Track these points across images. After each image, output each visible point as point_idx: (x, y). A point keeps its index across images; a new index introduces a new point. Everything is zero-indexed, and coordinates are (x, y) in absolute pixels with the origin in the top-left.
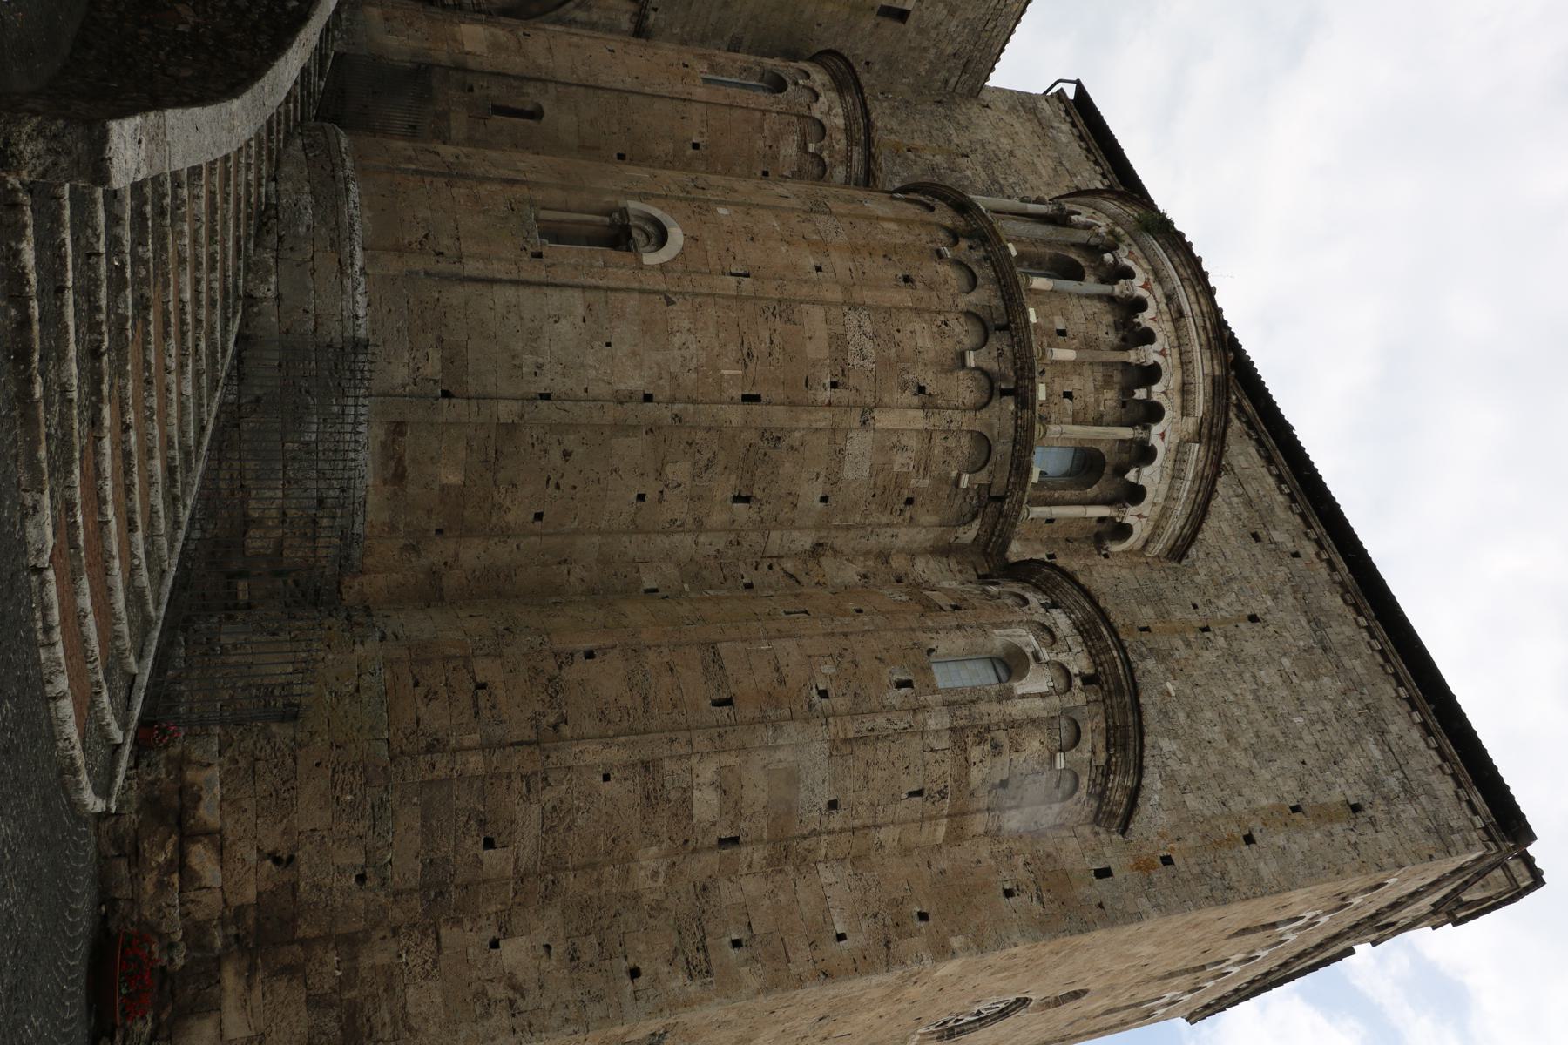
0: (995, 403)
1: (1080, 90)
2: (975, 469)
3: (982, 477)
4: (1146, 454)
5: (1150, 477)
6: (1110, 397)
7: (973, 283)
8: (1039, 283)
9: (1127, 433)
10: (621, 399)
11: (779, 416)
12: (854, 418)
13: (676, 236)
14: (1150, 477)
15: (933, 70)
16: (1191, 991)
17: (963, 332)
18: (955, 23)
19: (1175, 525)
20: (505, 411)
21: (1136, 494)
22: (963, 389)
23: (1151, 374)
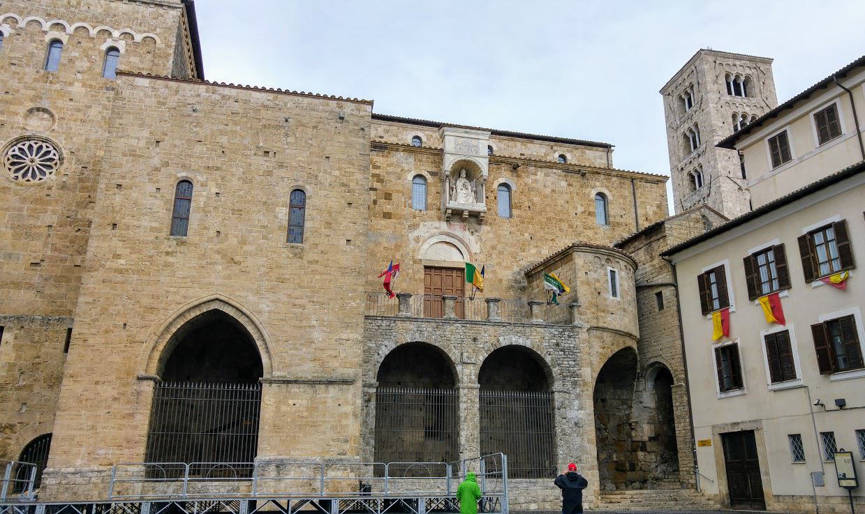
16: (110, 34)
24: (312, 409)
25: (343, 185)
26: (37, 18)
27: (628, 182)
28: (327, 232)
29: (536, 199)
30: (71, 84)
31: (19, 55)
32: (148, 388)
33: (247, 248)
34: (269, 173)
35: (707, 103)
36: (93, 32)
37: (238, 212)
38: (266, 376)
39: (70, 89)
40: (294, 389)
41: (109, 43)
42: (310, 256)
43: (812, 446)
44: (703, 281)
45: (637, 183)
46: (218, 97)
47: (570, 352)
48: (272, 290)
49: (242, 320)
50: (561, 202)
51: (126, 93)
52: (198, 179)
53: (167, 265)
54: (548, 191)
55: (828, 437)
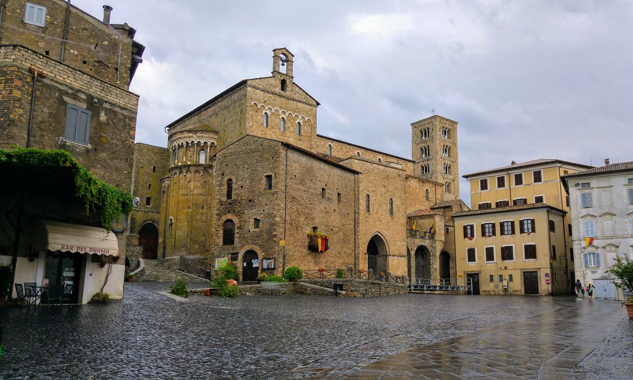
0: (191, 170)
1: (167, 127)
2: (200, 173)
3: (201, 171)
4: (199, 142)
5: (202, 142)
6: (191, 149)
7: (176, 173)
8: (176, 163)
9: (196, 146)
10: (188, 226)
11: (191, 204)
12: (192, 192)
13: (171, 217)
14: (202, 142)
15: (164, 159)
17: (182, 175)
18: (155, 158)
19: (211, 135)
20: (189, 240)
21: (206, 143)
22: (189, 175)
23: (187, 143)
24: (398, 263)
25: (401, 198)
26: (277, 109)
27: (434, 185)
28: (398, 212)
29: (411, 190)
30: (289, 138)
31: (274, 124)
32: (367, 256)
33: (383, 217)
34: (385, 193)
35: (436, 139)
36: (294, 116)
37: (380, 205)
38: (388, 254)
39: (290, 139)
40: (395, 258)
41: (298, 121)
42: (395, 220)
43: (496, 278)
44: (465, 228)
45: (437, 186)
46: (372, 167)
47: (434, 248)
48: (389, 229)
49: (382, 237)
50: (417, 192)
51: (353, 165)
52: (371, 194)
53: (367, 221)
54: (414, 187)
55: (501, 276)
